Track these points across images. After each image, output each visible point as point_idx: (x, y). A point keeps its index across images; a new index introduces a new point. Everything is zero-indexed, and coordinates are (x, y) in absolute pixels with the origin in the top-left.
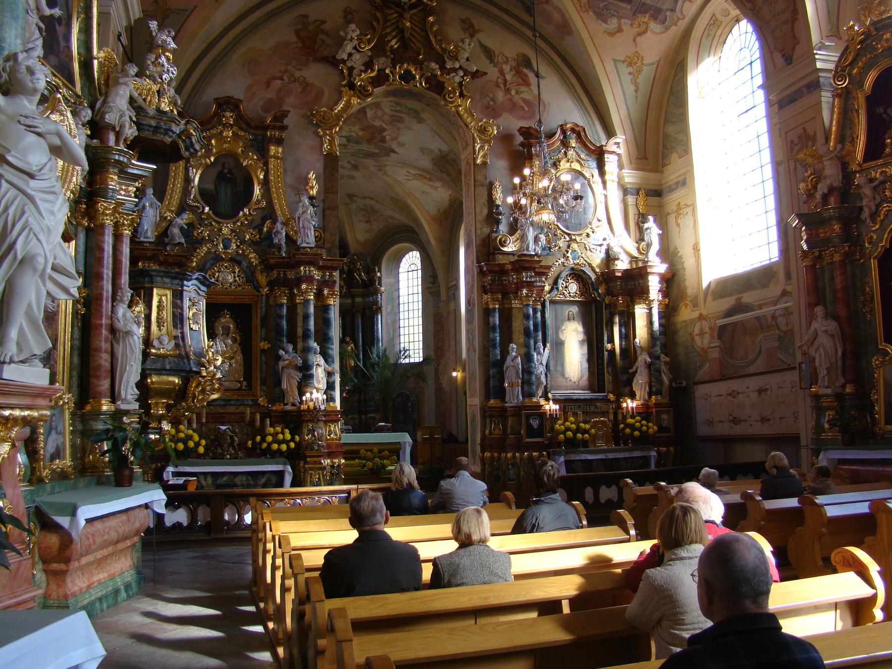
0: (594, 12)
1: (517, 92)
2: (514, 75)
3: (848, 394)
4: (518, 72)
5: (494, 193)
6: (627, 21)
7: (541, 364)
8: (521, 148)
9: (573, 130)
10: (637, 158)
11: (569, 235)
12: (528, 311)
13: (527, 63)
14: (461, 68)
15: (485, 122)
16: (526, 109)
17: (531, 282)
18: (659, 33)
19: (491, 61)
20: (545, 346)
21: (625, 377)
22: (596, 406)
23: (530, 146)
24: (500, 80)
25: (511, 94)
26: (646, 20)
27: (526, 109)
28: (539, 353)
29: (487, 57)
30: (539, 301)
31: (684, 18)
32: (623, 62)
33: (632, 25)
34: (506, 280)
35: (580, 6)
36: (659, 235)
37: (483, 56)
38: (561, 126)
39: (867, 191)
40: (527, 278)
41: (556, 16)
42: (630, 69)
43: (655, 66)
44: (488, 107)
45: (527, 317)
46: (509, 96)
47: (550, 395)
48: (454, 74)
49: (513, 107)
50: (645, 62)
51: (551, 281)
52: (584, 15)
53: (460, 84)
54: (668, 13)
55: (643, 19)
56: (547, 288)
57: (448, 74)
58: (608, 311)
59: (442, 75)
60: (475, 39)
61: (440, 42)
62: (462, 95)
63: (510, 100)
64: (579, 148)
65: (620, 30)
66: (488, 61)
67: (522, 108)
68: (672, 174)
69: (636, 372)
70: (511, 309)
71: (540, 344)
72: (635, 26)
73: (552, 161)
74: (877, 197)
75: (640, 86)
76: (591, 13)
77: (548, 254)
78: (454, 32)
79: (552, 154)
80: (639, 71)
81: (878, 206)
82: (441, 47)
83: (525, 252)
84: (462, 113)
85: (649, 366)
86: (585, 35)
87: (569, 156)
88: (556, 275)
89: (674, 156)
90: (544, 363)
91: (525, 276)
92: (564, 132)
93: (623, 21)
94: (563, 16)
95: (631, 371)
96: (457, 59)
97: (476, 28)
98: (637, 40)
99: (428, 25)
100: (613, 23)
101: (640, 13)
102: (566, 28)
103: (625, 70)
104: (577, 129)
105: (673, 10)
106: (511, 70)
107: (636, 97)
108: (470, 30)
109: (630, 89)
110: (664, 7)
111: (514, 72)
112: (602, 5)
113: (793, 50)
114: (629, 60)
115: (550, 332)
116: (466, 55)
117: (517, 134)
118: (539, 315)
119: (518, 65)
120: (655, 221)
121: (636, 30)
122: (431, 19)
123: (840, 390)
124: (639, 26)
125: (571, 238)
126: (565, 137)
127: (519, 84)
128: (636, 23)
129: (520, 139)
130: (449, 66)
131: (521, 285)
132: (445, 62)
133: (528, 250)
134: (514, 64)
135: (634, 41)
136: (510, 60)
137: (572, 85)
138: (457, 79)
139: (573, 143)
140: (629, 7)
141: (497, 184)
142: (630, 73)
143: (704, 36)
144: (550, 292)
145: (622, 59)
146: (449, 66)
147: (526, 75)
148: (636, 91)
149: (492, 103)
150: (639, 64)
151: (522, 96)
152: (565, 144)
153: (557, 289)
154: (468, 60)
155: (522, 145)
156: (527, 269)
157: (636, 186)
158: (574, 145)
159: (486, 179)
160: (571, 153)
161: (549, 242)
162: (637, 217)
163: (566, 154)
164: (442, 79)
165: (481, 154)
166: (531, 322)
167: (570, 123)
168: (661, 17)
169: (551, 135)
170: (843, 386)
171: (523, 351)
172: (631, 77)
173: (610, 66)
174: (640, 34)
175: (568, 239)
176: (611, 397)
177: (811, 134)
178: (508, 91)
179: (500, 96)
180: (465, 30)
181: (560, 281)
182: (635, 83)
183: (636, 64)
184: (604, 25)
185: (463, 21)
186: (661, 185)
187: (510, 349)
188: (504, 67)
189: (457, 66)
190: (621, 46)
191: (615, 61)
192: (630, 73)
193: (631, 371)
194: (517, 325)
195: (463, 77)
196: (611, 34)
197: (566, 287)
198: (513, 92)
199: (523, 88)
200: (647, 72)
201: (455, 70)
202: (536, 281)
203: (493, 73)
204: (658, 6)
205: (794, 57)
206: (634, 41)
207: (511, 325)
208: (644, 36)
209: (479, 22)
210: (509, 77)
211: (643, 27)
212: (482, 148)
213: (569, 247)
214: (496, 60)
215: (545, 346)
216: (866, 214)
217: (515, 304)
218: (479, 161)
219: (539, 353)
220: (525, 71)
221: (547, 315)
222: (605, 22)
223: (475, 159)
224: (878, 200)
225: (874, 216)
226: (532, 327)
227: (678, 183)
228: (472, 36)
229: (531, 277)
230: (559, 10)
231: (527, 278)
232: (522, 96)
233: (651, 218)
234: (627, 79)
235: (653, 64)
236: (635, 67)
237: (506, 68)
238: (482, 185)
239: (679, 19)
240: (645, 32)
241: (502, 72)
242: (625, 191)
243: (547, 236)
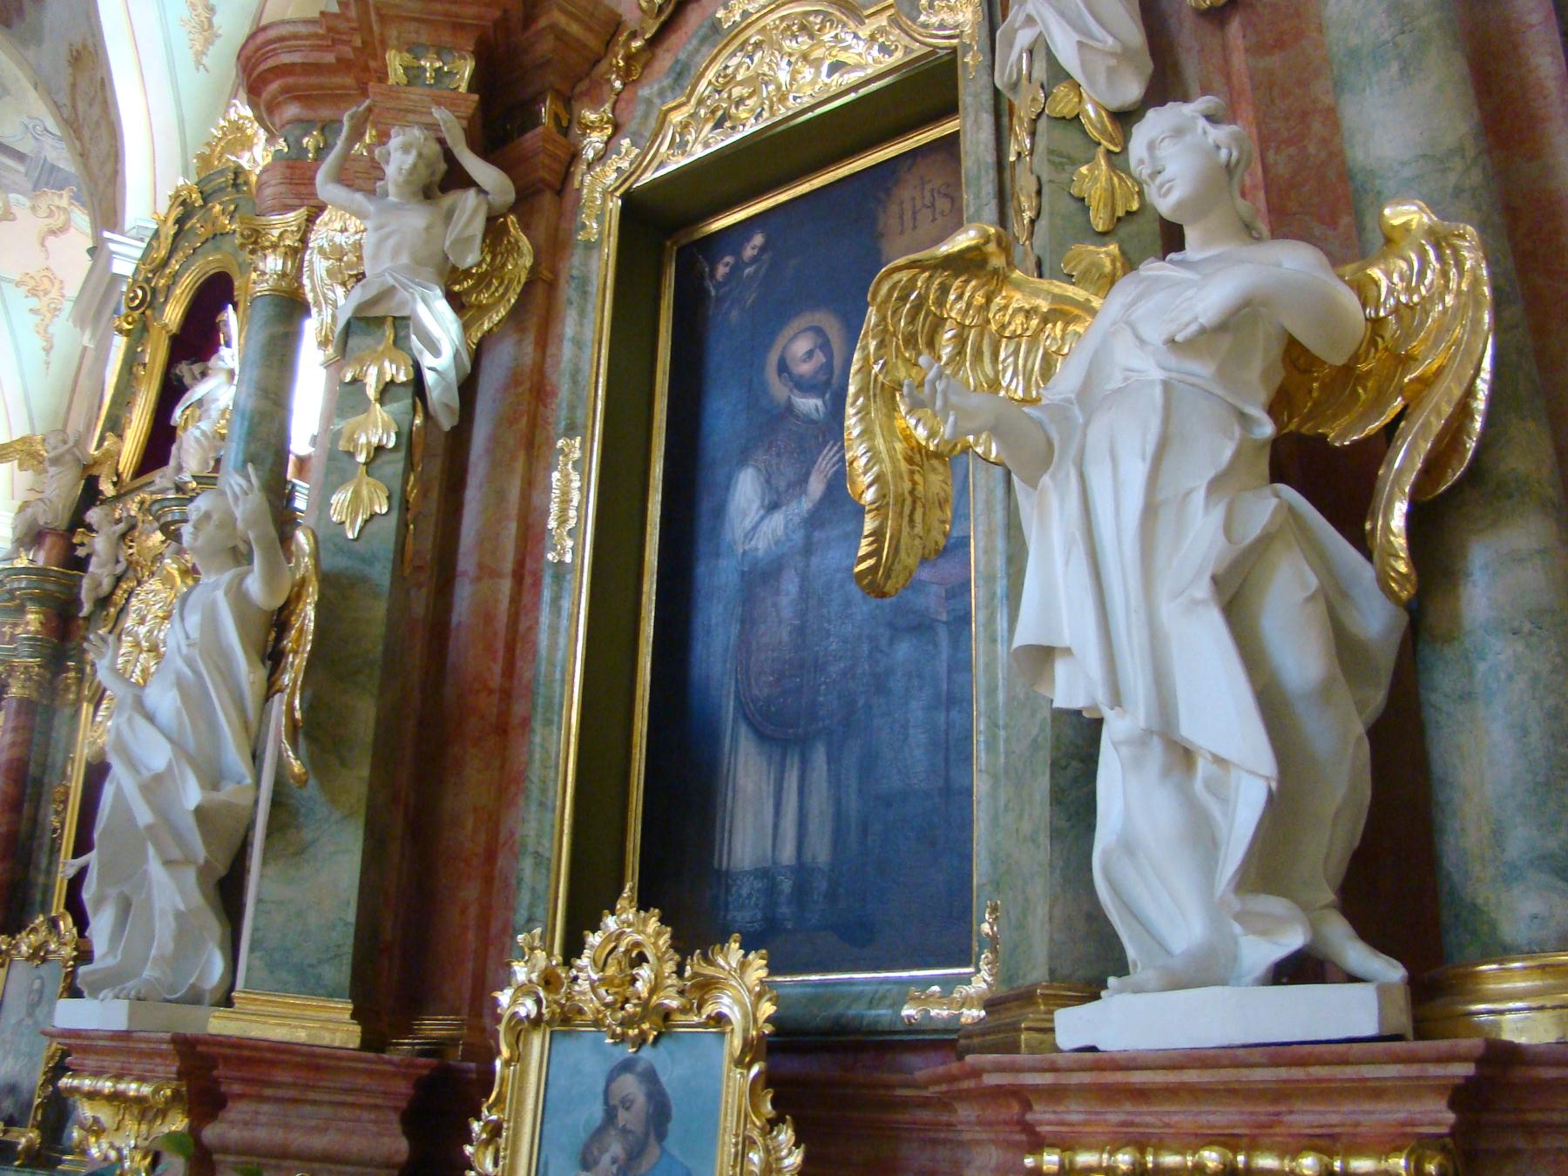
6: (20, 197)
26: (64, 202)
32: (18, 284)
33: (33, 208)
42: (33, 302)
55: (57, 201)
72: (43, 211)
75: (56, 341)
98: (47, 243)
101: (47, 185)
107: (48, 363)
109: (33, 344)
114: (32, 283)
121: (43, 223)
124: (51, 215)
128: (43, 204)
135: (43, 245)
140: (21, 168)
148: (48, 350)
150: (54, 294)
172: (37, 319)
174: (53, 232)
182: (44, 332)
183: (46, 293)
206: (43, 245)
211: (58, 221)
224: (120, 568)
236: (45, 300)
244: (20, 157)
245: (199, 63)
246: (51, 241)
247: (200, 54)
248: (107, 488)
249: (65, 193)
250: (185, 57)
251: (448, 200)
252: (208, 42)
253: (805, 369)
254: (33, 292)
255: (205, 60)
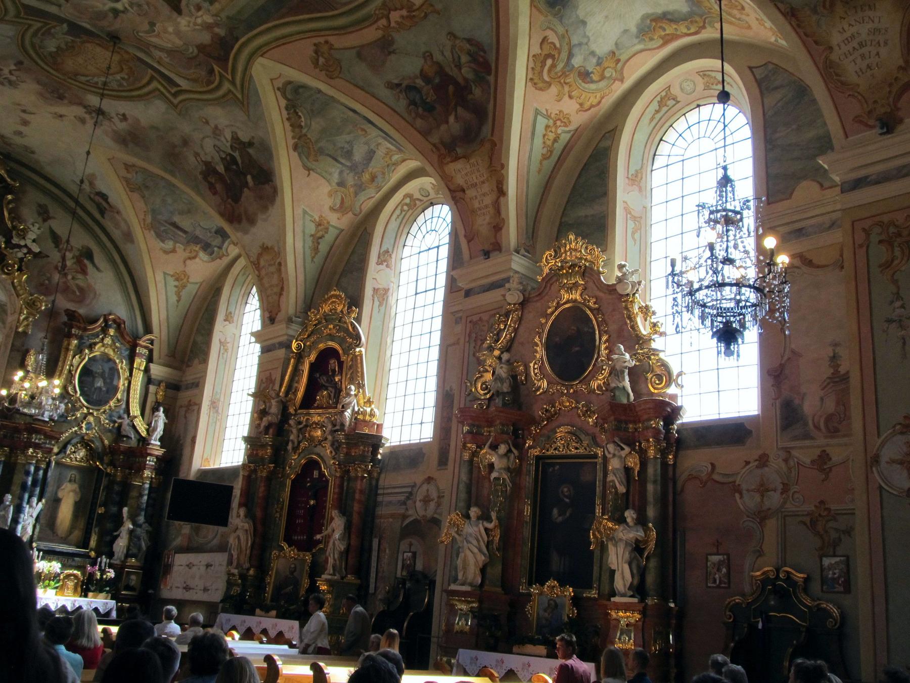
0: (155, 232)
1: (73, 278)
2: (75, 263)
3: (250, 576)
4: (79, 261)
5: (28, 358)
6: (181, 246)
7: (31, 516)
8: (63, 326)
9: (114, 321)
10: (167, 355)
11: (87, 408)
12: (29, 468)
13: (89, 255)
14: (26, 246)
15: (36, 297)
16: (78, 293)
17: (38, 444)
18: (206, 262)
19: (57, 246)
20: (39, 500)
21: (108, 538)
22: (73, 560)
23: (71, 327)
24: (60, 264)
25: (66, 278)
26: (197, 249)
27: (78, 293)
28: (31, 506)
29: (54, 242)
30: (44, 461)
31: (228, 255)
33: (185, 250)
34: (17, 437)
35: (144, 224)
36: (165, 424)
37: (50, 241)
38: (105, 315)
39: (295, 431)
40: (35, 439)
41: (123, 225)
42: (176, 283)
43: (197, 286)
44: (42, 285)
45: (27, 473)
46: (64, 280)
47: (34, 545)
48: (18, 250)
49: (66, 290)
50: (191, 280)
51: (61, 445)
52: (146, 232)
53: (21, 260)
54: (216, 249)
55: (194, 248)
56: (56, 450)
57: (12, 249)
58: (107, 479)
59: (6, 248)
60: (47, 224)
61: (12, 220)
62: (20, 269)
63: (65, 283)
64: (116, 336)
65: (174, 251)
66: (52, 245)
67: (74, 292)
68: (189, 377)
69: (118, 535)
70: (15, 464)
71: (35, 500)
72: (187, 251)
73: (88, 343)
74: (301, 436)
75: (183, 298)
76: (152, 232)
77: (64, 422)
78: (28, 213)
79: (91, 337)
80: (184, 287)
81: (299, 443)
82: (12, 223)
83: (40, 418)
84: (16, 285)
85: (131, 532)
86: (143, 246)
87: (105, 342)
88: (68, 440)
89: (196, 361)
90: (35, 515)
91: (35, 439)
92: (106, 321)
93: (178, 245)
94: (129, 228)
95: (115, 534)
96: (24, 238)
97: (51, 215)
99: (5, 202)
100: (169, 245)
101: (193, 242)
102: (129, 236)
103: (172, 283)
104: (118, 321)
105: (220, 248)
106: (73, 258)
108: (44, 214)
109: (173, 299)
110: (214, 243)
111: (75, 260)
112: (163, 228)
113: (277, 314)
114: (177, 276)
115: (50, 489)
116: (34, 236)
117: (63, 314)
118: (41, 472)
119: (81, 255)
120: (164, 412)
121: (187, 254)
122: (10, 197)
123: (245, 572)
124: (191, 252)
125: (88, 411)
126: (105, 326)
127: (77, 272)
128: (189, 249)
129: (65, 319)
130: (15, 241)
131: (29, 444)
132: (12, 238)
133: (43, 415)
134: (77, 253)
135: (184, 262)
136: (74, 249)
137: (125, 283)
138: (20, 255)
139: (112, 332)
140: (185, 236)
141: (32, 352)
142: (176, 286)
143: (240, 274)
144: (57, 454)
145: (172, 273)
146: (15, 241)
147: (85, 265)
148: (178, 301)
149: (47, 282)
150: (185, 280)
151: (77, 282)
152: (105, 330)
153: (65, 453)
154: (34, 241)
155: (65, 324)
156: (38, 432)
157: (159, 378)
158: (112, 334)
159: (23, 346)
160: (108, 341)
161: (67, 410)
162: (153, 404)
163: (103, 339)
164: (5, 252)
165: (25, 323)
166: (30, 479)
167: (114, 314)
168: (209, 250)
169: (95, 321)
170: (248, 569)
171: (17, 501)
173: (160, 277)
174: (190, 258)
175: (85, 411)
176: (93, 554)
177: (273, 378)
178: (65, 275)
179: (56, 277)
180: (39, 214)
181: (69, 447)
183: (182, 280)
184: (161, 244)
185: (40, 206)
186: (181, 381)
187: (5, 498)
188: (67, 254)
189: (22, 243)
190: (174, 263)
191: (165, 273)
192: (176, 286)
193: (115, 534)
194: (17, 479)
195: (25, 254)
196: (166, 252)
197: (74, 452)
198: (70, 277)
199: (80, 276)
200: (191, 289)
201: (19, 246)
202: (45, 443)
203: (55, 256)
204: (209, 241)
205: (276, 320)
206: (184, 262)
207: (12, 478)
208: (193, 260)
209: (53, 209)
210: (69, 263)
211: (193, 255)
212: (26, 319)
213: (85, 418)
214: (61, 247)
215: (39, 500)
216: (290, 447)
217: (21, 459)
218: (20, 330)
219: (31, 506)
220: (86, 261)
221: (49, 474)
222: (163, 241)
223: (17, 327)
225: (295, 449)
226: (30, 483)
227: (193, 383)
228: (45, 220)
229: (40, 439)
230: (126, 222)
231: (35, 439)
232: (77, 282)
233: (162, 409)
234: (172, 290)
235: (197, 283)
236: (181, 282)
237: (69, 255)
238: (18, 351)
239: (224, 255)
240: (194, 258)
241: (64, 258)
242: (149, 381)
243: (66, 405)
244: (185, 232)
245: (312, 260)
246: (188, 262)
247: (313, 258)
248: (292, 410)
249: (199, 246)
250: (309, 259)
251: (509, 454)
252: (316, 254)
253: (566, 494)
254: (177, 280)
255: (315, 260)
